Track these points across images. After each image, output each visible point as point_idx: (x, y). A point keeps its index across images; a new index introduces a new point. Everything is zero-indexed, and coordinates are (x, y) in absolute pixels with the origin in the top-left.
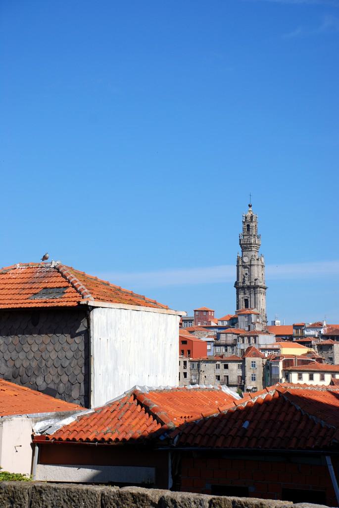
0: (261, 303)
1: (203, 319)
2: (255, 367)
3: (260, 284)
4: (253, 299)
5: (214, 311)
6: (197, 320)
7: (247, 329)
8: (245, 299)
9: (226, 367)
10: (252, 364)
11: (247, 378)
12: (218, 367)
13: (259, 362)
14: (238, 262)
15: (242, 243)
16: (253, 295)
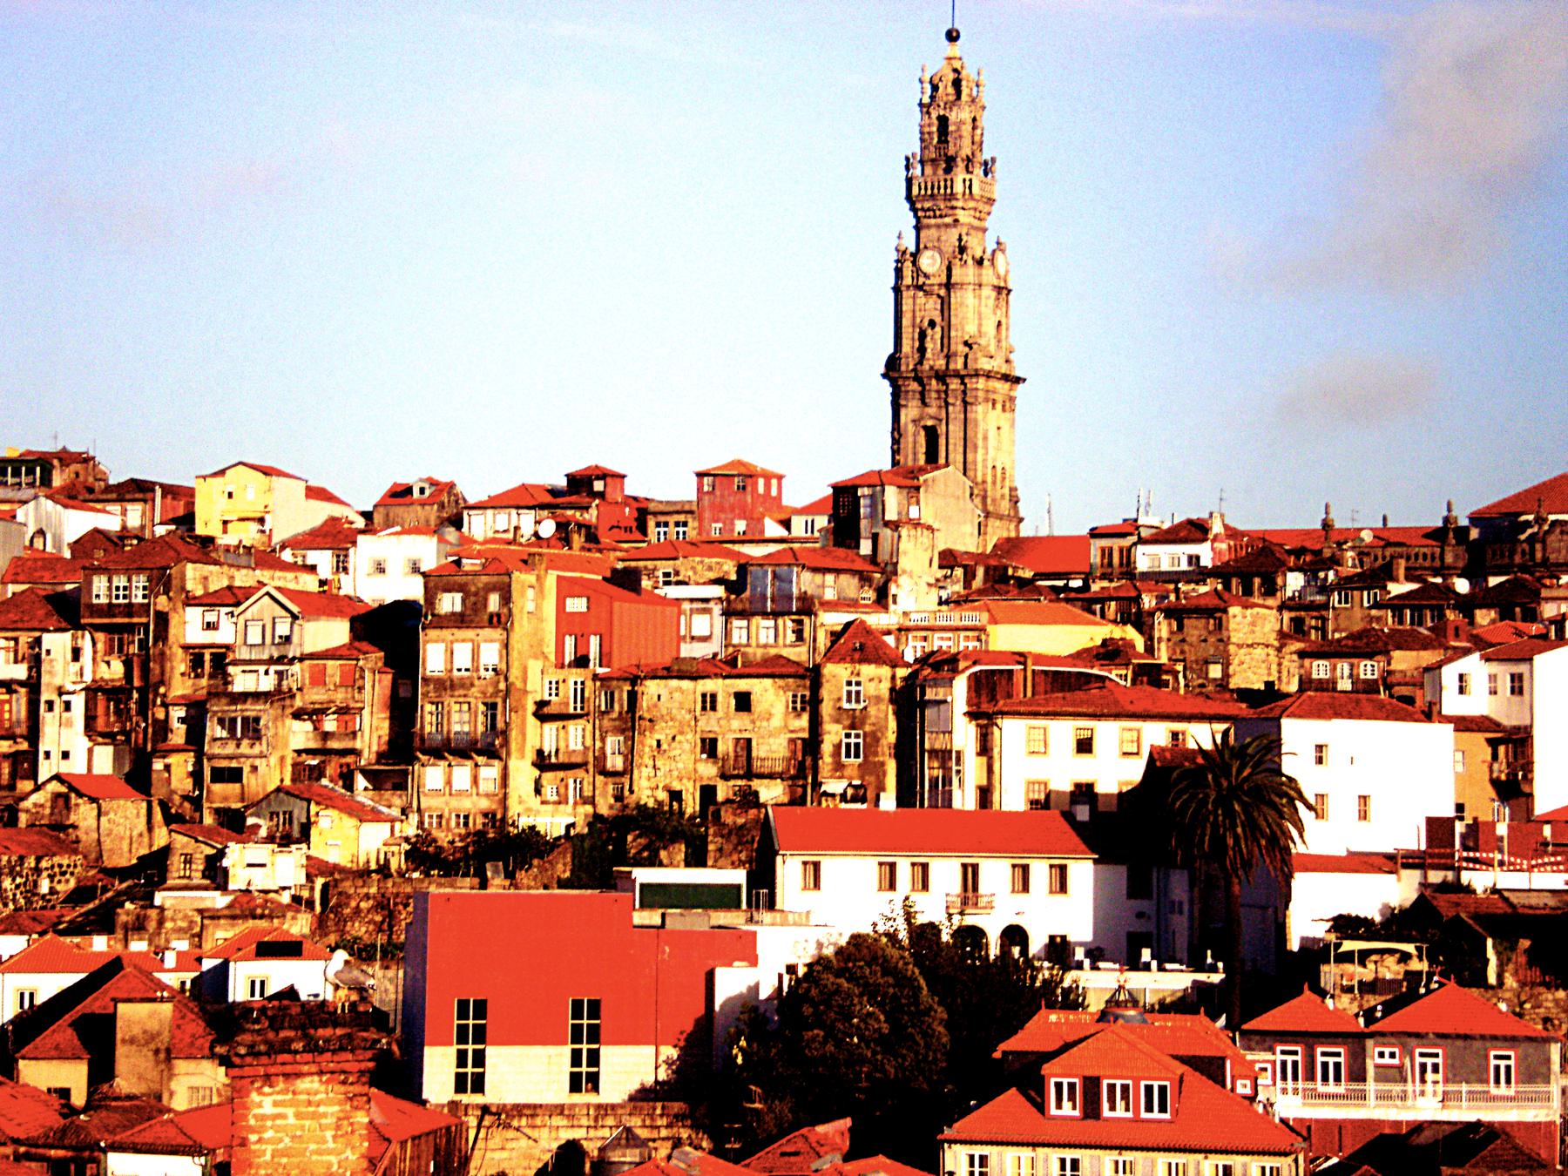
0: (992, 442)
1: (732, 510)
2: (858, 701)
3: (985, 364)
4: (956, 430)
5: (780, 478)
6: (707, 515)
8: (925, 428)
9: (743, 702)
10: (849, 693)
11: (827, 748)
12: (710, 702)
13: (876, 680)
14: (899, 272)
15: (915, 191)
16: (956, 411)
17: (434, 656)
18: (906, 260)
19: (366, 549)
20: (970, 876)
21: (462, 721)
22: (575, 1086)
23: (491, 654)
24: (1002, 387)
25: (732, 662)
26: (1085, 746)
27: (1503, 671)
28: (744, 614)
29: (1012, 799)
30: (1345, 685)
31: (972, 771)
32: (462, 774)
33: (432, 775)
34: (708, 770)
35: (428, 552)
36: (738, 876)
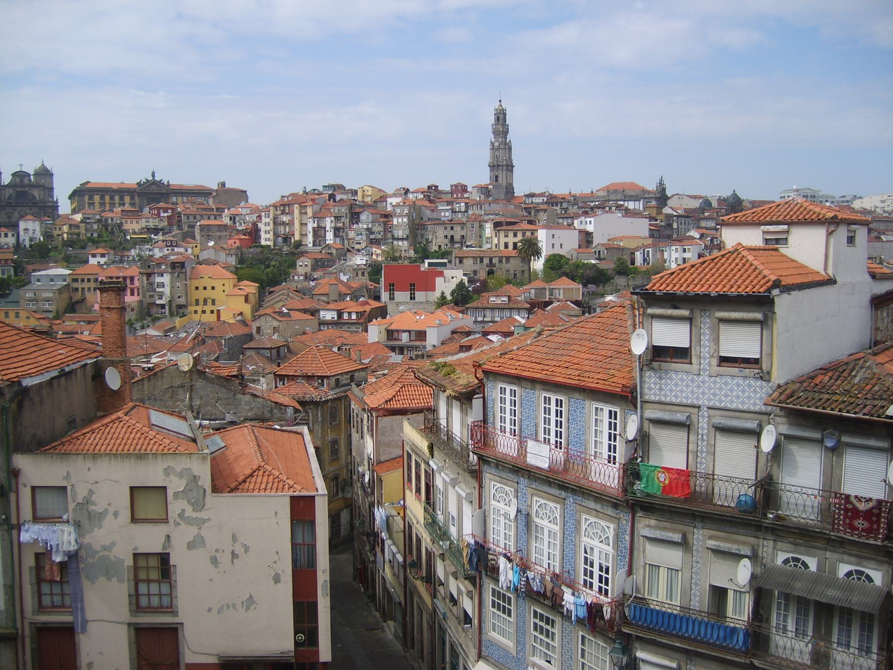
7: (478, 199)
9: (452, 228)
12: (446, 228)
17: (395, 221)
18: (492, 144)
19: (389, 200)
20: (491, 260)
21: (400, 233)
22: (411, 299)
23: (405, 220)
24: (510, 168)
25: (451, 220)
26: (515, 235)
27: (588, 220)
28: (455, 212)
29: (502, 247)
30: (565, 223)
31: (495, 241)
32: (400, 243)
33: (395, 242)
34: (446, 241)
35: (399, 200)
36: (446, 261)
